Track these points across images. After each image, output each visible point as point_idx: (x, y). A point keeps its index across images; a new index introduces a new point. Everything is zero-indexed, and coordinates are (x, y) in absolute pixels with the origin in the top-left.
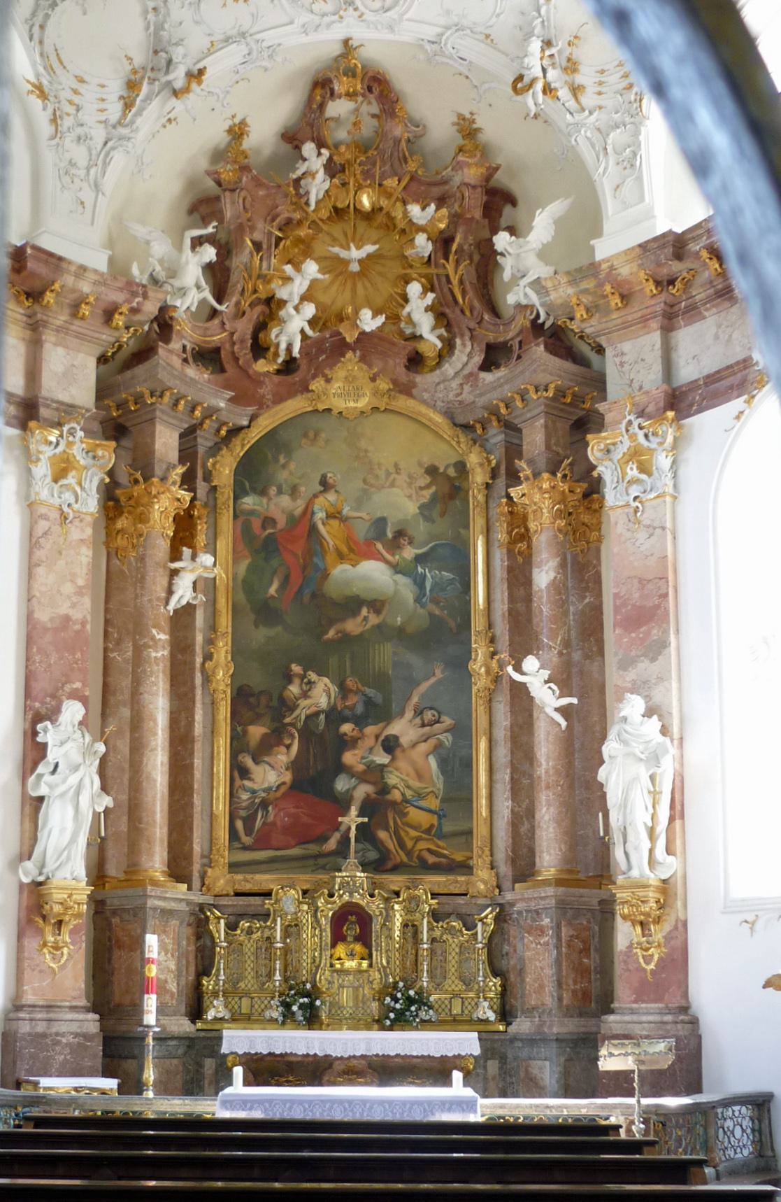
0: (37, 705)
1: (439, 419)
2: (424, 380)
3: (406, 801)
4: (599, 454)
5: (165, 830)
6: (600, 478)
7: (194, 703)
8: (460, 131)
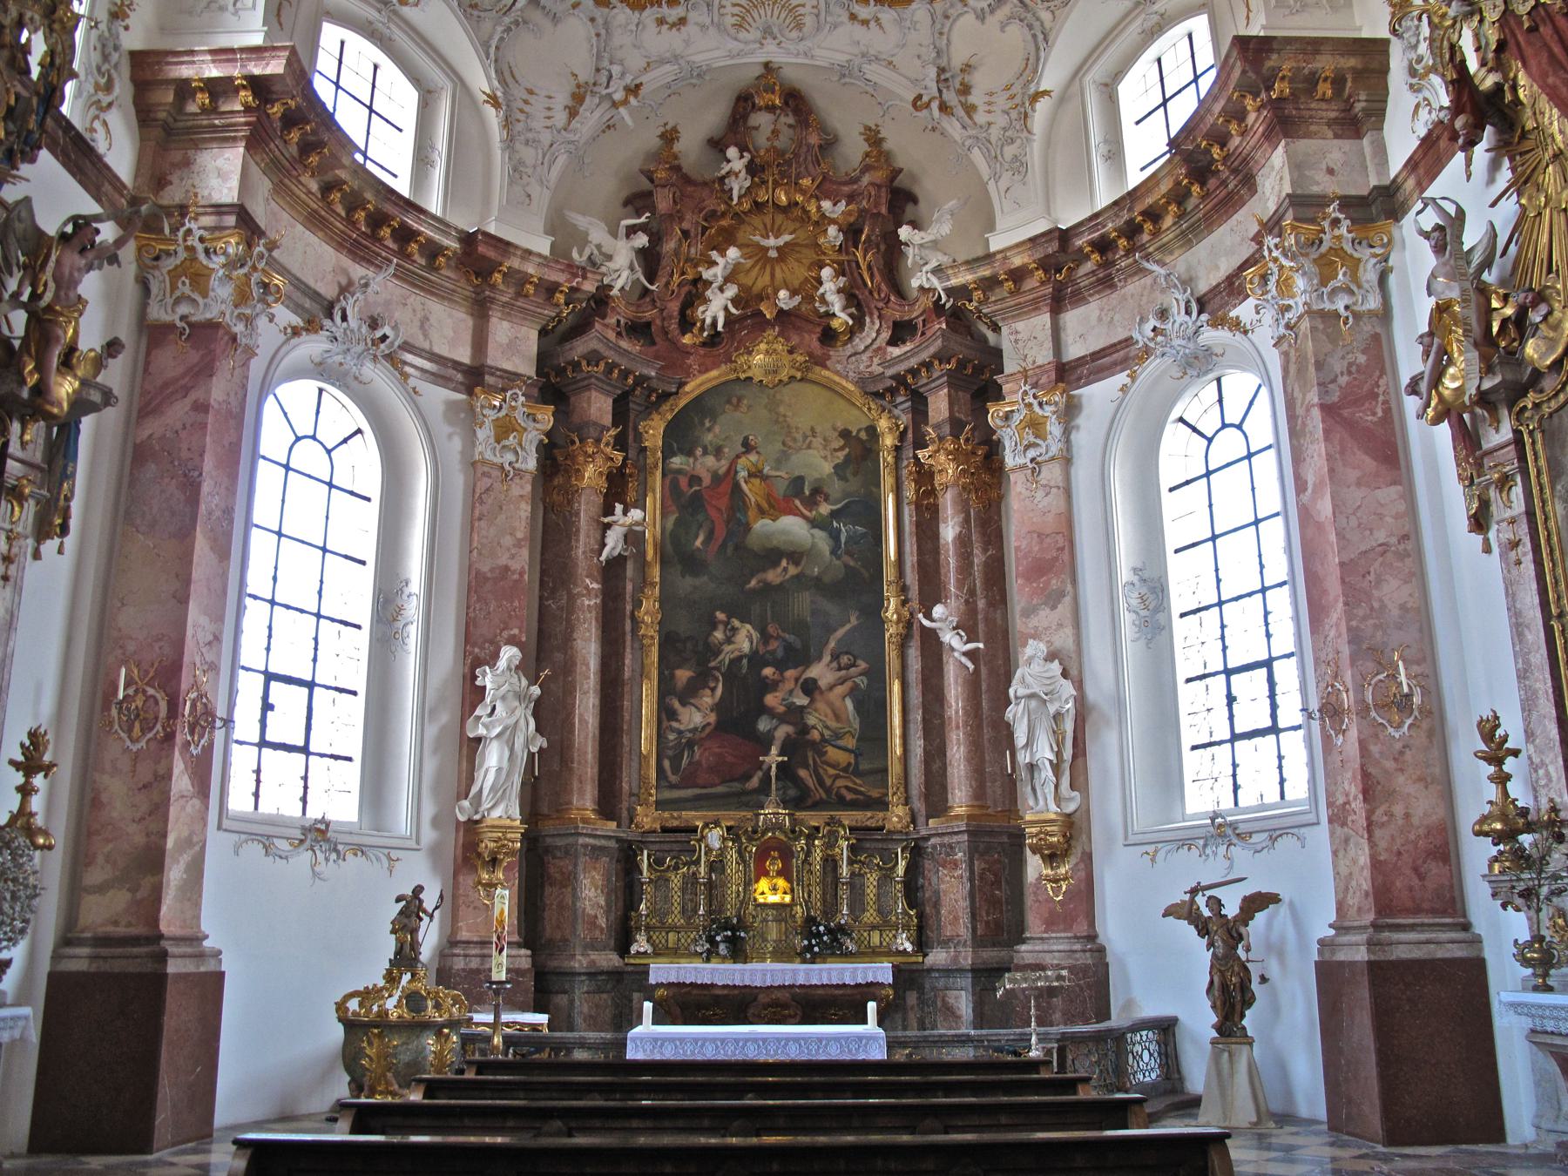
0: (477, 650)
1: (851, 387)
2: (839, 354)
3: (824, 740)
4: (999, 422)
5: (596, 770)
6: (999, 441)
7: (624, 648)
8: (866, 140)
